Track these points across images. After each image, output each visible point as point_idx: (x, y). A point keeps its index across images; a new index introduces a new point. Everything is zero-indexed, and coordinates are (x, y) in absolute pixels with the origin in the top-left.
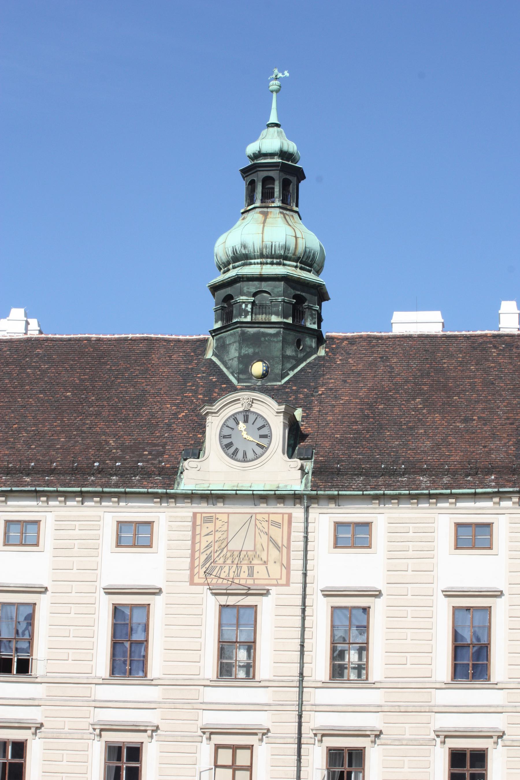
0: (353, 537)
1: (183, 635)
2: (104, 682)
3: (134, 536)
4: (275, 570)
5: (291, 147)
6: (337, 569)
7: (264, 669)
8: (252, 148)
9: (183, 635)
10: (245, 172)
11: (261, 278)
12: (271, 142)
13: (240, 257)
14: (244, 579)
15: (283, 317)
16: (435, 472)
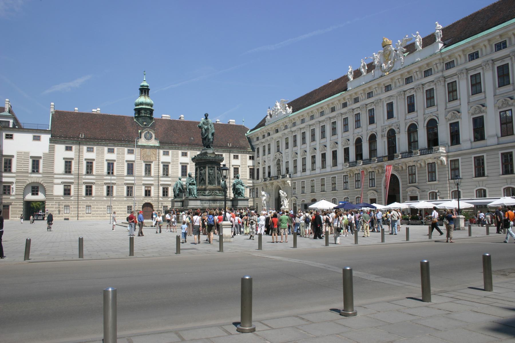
0: (166, 154)
1: (140, 168)
2: (127, 176)
3: (131, 152)
4: (154, 158)
5: (148, 85)
6: (164, 159)
7: (152, 174)
8: (142, 84)
9: (140, 168)
10: (140, 89)
11: (146, 108)
12: (145, 84)
13: (142, 104)
14: (149, 160)
15: (144, 114)
16: (179, 144)
